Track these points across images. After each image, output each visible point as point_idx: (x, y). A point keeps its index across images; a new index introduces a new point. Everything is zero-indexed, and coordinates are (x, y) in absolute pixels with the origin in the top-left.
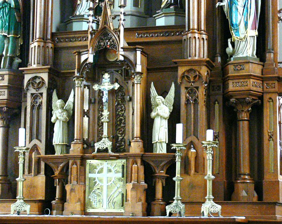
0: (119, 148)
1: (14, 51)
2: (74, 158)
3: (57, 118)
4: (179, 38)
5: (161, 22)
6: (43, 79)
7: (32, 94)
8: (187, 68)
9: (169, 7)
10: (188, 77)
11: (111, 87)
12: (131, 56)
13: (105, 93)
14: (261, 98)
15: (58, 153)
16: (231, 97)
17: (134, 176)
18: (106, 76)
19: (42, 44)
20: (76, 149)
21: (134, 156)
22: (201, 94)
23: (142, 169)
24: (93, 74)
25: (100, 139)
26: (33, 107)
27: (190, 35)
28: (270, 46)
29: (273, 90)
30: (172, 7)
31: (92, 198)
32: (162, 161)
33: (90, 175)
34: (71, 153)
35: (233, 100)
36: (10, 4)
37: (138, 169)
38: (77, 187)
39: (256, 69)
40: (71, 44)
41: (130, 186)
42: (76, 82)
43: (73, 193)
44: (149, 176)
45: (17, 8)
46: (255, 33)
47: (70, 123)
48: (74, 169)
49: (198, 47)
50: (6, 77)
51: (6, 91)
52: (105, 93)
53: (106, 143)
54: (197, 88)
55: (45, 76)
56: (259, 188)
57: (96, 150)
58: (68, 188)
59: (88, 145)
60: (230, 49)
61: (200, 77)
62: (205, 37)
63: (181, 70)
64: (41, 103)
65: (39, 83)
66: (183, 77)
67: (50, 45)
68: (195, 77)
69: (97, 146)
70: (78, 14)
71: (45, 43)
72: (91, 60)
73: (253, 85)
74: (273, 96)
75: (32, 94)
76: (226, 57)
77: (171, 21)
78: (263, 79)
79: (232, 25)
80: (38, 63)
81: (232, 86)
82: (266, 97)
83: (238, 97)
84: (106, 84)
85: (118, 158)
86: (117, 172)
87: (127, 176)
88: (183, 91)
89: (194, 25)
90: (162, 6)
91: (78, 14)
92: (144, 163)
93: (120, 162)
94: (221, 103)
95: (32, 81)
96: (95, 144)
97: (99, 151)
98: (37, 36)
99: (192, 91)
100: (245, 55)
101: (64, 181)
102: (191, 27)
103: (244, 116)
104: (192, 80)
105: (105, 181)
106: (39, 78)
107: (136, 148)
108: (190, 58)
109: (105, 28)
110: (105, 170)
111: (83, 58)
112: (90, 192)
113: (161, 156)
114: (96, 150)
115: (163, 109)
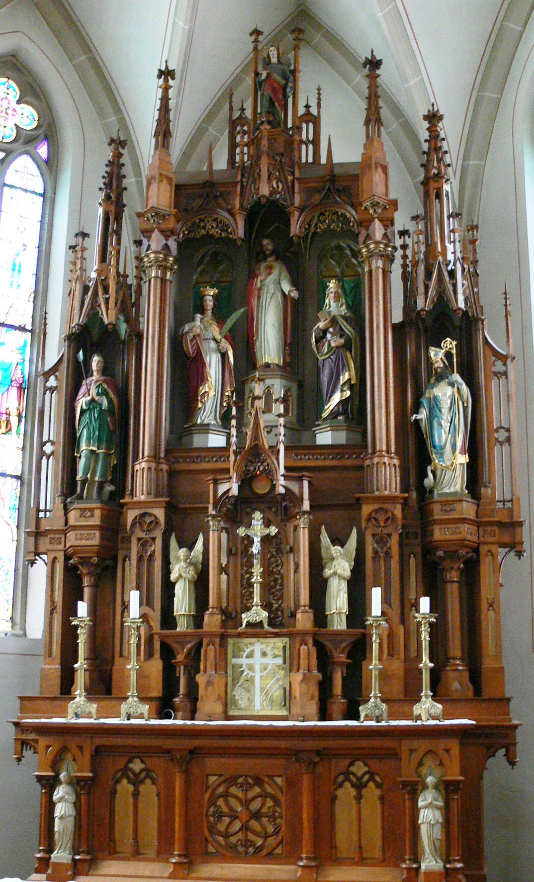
0: (279, 623)
1: (103, 475)
2: (211, 635)
3: (181, 576)
4: (356, 462)
5: (325, 437)
6: (156, 518)
7: (139, 539)
8: (376, 506)
9: (336, 417)
10: (376, 519)
11: (267, 531)
12: (295, 487)
13: (257, 540)
14: (476, 550)
15: (182, 626)
16: (437, 548)
17: (303, 662)
18: (258, 515)
19: (153, 465)
20: (212, 621)
21: (304, 634)
22: (394, 542)
23: (314, 651)
24: (235, 512)
25: (248, 609)
26: (140, 559)
27: (376, 460)
28: (486, 478)
29: (493, 539)
30: (340, 418)
31: (239, 695)
32: (341, 642)
33: (235, 661)
34: (206, 628)
35: (440, 553)
36: (101, 405)
37: (307, 651)
38: (216, 678)
39: (468, 509)
40: (193, 466)
41: (298, 677)
42: (211, 523)
43: (210, 688)
44: (324, 661)
45: (110, 411)
46: (464, 459)
47: (200, 584)
48: (209, 652)
49: (387, 476)
50: (98, 513)
51: (97, 533)
52: (257, 540)
53: (257, 614)
54: (389, 535)
55: (160, 513)
56: (475, 676)
57: (244, 626)
58: (201, 679)
59: (230, 617)
60: (429, 481)
61: (394, 518)
62: (396, 462)
63: (366, 509)
64: (154, 552)
65: (151, 522)
66: (369, 519)
67: (165, 467)
68: (387, 519)
69: (245, 618)
70: (199, 422)
71: (158, 463)
72: (235, 491)
73: (467, 532)
74: (494, 548)
75: (139, 539)
76: (425, 494)
77: (342, 438)
78: (478, 524)
79: (434, 447)
80: (149, 494)
81: (439, 534)
82: (484, 549)
83: (447, 549)
84: (257, 528)
85: (277, 635)
86: (275, 656)
87: (291, 663)
88: (369, 539)
89: (382, 445)
90: (325, 415)
91: (199, 422)
92: (316, 643)
93: (280, 642)
94: (419, 556)
95: (139, 520)
96: (243, 616)
97: (249, 624)
98: (146, 454)
99: (382, 540)
100: (452, 490)
101: (193, 667)
102: (378, 448)
103: (454, 575)
104: (382, 524)
105: (257, 667)
106: (151, 515)
107: (304, 620)
108: (377, 493)
109: (256, 445)
110: (257, 654)
111: (222, 488)
112: (234, 685)
113: (339, 633)
114: (244, 626)
115: (340, 565)
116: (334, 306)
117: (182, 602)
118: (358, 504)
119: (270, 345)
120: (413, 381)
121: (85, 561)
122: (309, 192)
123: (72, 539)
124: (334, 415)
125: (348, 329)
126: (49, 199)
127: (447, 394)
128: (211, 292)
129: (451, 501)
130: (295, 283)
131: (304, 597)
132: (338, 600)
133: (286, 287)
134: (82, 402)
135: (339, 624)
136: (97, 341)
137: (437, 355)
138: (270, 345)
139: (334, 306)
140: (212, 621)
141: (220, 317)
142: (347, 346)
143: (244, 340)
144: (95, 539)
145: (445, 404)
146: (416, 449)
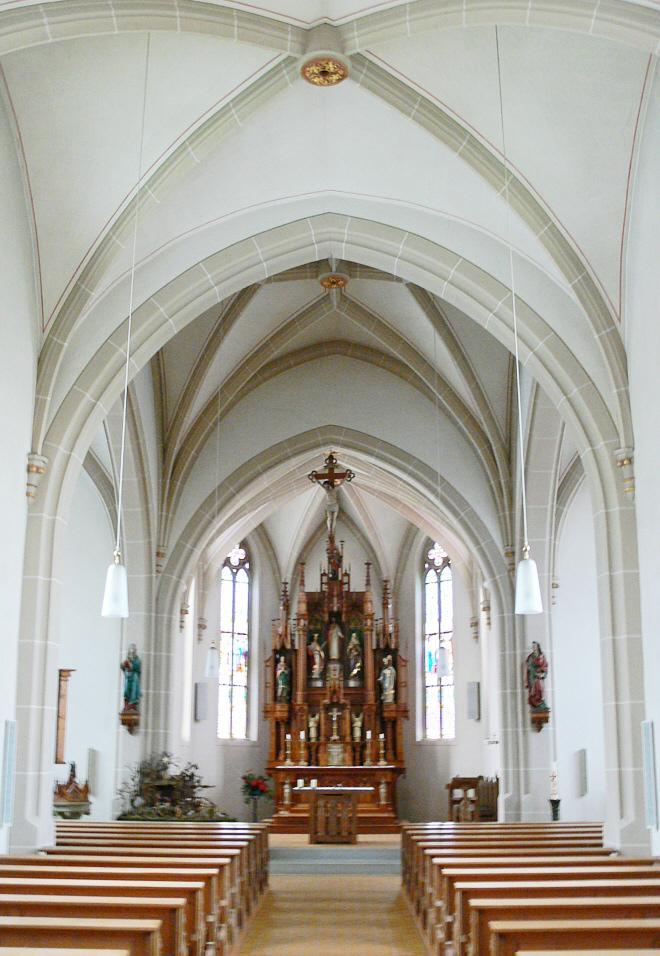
0: (342, 739)
5: (352, 684)
15: (313, 741)
20: (322, 739)
22: (373, 717)
24: (328, 708)
25: (332, 735)
37: (349, 748)
41: (347, 755)
44: (354, 750)
47: (318, 729)
48: (321, 749)
53: (335, 737)
55: (305, 708)
56: (395, 754)
58: (320, 755)
59: (328, 739)
60: (382, 698)
73: (394, 714)
76: (382, 702)
78: (397, 711)
81: (386, 715)
84: (335, 714)
87: (345, 751)
99: (369, 716)
101: (317, 751)
107: (348, 739)
115: (358, 724)
116: (354, 640)
117: (313, 733)
118: (362, 705)
119: (335, 653)
120: (379, 667)
121: (283, 721)
122: (347, 607)
123: (278, 714)
124: (355, 675)
125: (359, 649)
126: (250, 584)
127: (389, 672)
128: (316, 635)
129: (389, 704)
130: (343, 633)
131: (348, 732)
132: (358, 733)
133: (340, 634)
134: (279, 672)
135: (358, 740)
136: (283, 652)
137: (385, 660)
138: (335, 653)
139: (354, 640)
140: (322, 739)
141: (320, 643)
142: (358, 655)
143: (327, 650)
144: (286, 715)
145: (388, 676)
146: (379, 688)
